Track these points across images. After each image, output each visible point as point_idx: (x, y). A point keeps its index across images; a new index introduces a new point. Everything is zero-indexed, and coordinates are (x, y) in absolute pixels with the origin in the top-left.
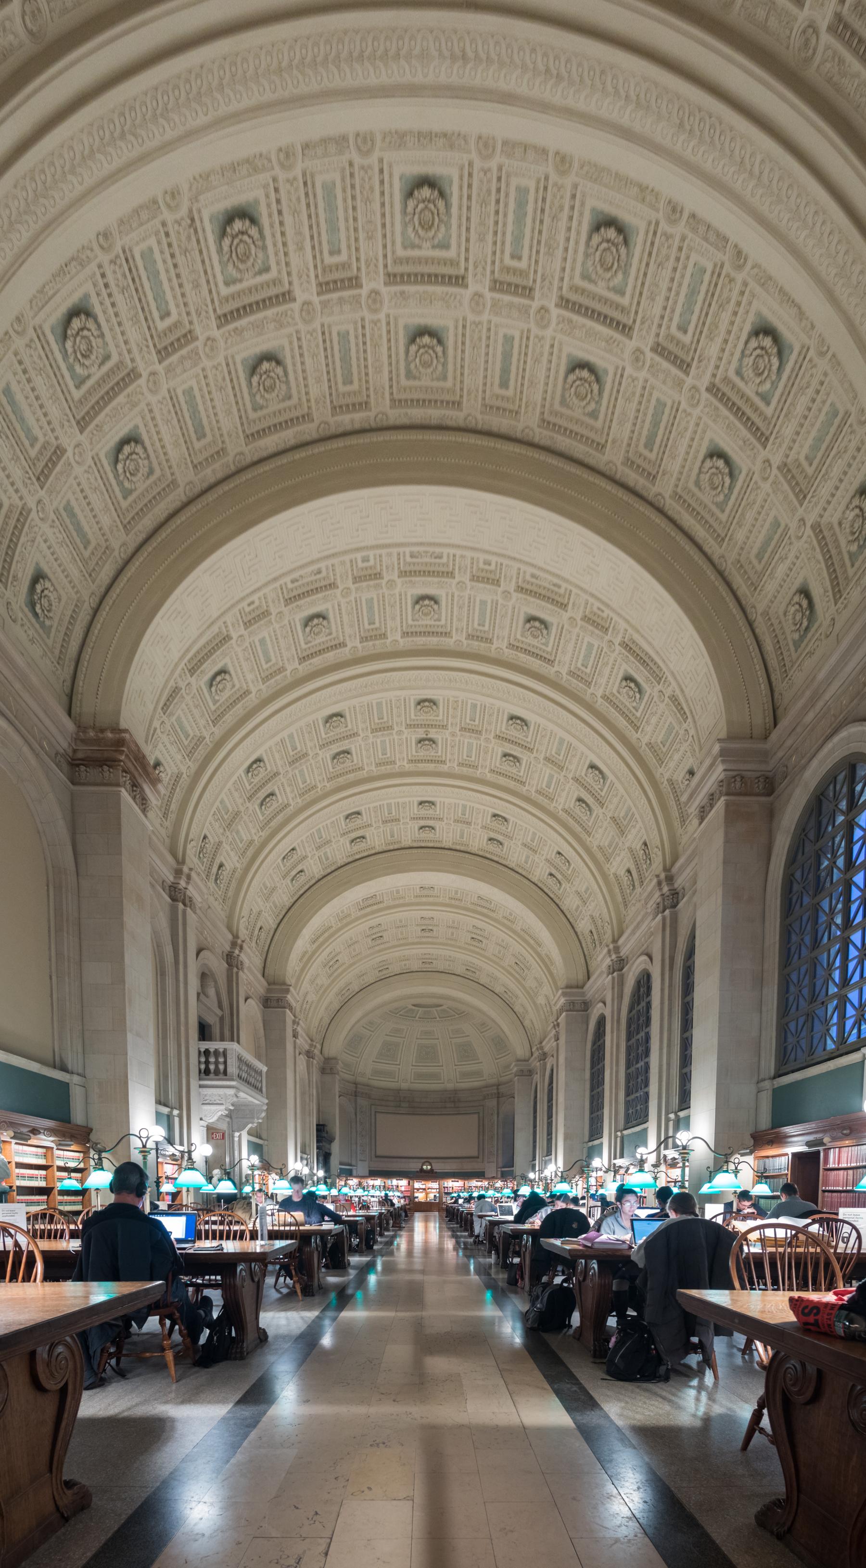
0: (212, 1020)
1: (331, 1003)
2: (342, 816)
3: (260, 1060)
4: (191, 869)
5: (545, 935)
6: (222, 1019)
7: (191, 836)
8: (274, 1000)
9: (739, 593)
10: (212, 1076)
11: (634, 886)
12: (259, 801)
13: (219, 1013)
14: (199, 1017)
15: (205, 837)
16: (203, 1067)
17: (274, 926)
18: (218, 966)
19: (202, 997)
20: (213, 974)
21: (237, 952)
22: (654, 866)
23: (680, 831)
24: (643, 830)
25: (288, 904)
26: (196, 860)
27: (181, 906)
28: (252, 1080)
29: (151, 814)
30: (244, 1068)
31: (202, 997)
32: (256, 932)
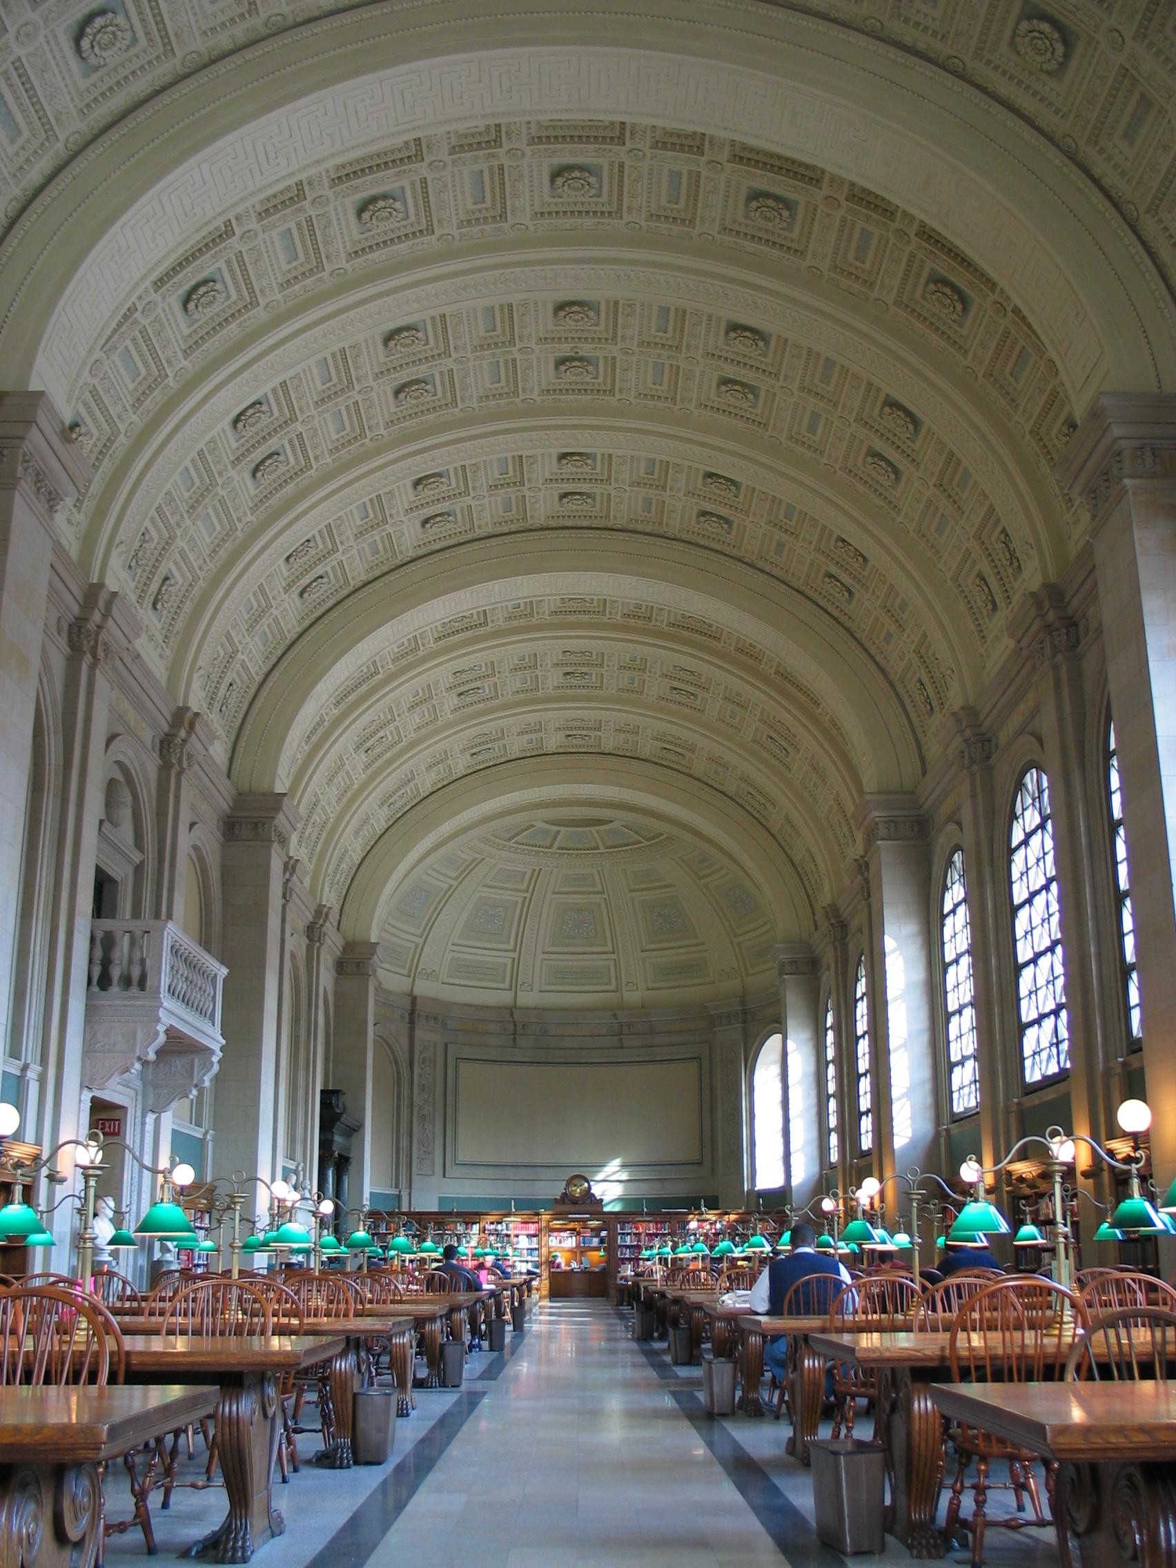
0: (121, 871)
1: (366, 820)
2: (408, 482)
3: (208, 949)
5: (824, 684)
6: (139, 869)
7: (120, 536)
8: (251, 821)
9: (1107, 182)
10: (115, 989)
11: (994, 604)
13: (137, 857)
14: (97, 866)
16: (97, 971)
17: (258, 679)
18: (147, 766)
19: (106, 824)
20: (130, 781)
22: (1026, 573)
25: (290, 637)
26: (125, 575)
28: (196, 996)
30: (183, 969)
31: (106, 824)
32: (222, 692)
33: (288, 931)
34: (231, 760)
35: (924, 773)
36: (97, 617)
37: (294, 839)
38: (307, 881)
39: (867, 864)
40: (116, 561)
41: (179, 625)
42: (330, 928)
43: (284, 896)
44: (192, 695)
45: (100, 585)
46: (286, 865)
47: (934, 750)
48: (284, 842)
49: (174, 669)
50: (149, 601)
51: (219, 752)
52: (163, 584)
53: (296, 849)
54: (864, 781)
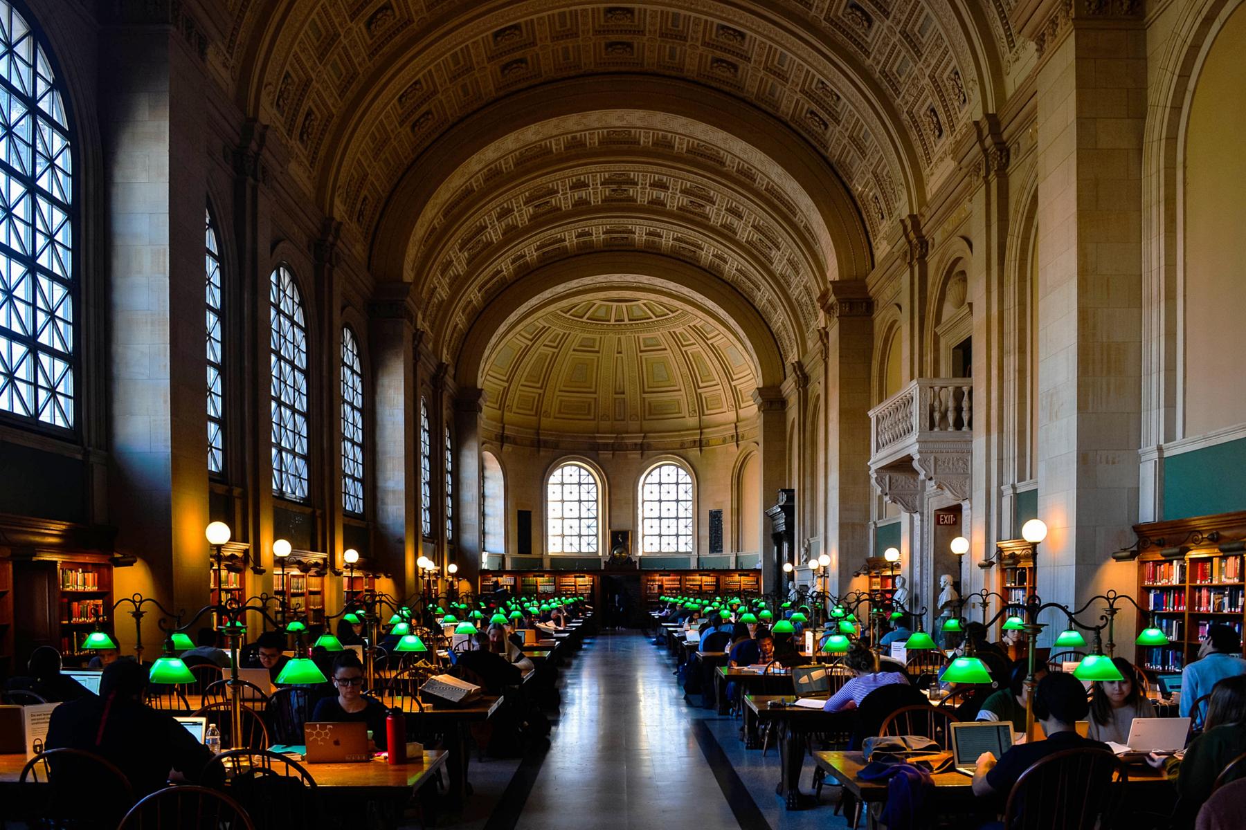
4: (266, 127)
12: (366, 18)
15: (287, 75)
21: (331, 239)
23: (1008, 56)
24: (951, 52)
27: (251, 180)
29: (211, 52)
32: (358, 206)
33: (419, 382)
34: (370, 258)
35: (873, 267)
36: (254, 146)
37: (420, 316)
38: (430, 346)
39: (827, 334)
40: (265, 100)
41: (322, 153)
42: (449, 381)
43: (415, 358)
44: (335, 210)
45: (255, 119)
46: (414, 335)
47: (882, 250)
48: (413, 319)
49: (320, 188)
50: (297, 132)
51: (359, 250)
52: (306, 119)
53: (423, 324)
54: (828, 275)
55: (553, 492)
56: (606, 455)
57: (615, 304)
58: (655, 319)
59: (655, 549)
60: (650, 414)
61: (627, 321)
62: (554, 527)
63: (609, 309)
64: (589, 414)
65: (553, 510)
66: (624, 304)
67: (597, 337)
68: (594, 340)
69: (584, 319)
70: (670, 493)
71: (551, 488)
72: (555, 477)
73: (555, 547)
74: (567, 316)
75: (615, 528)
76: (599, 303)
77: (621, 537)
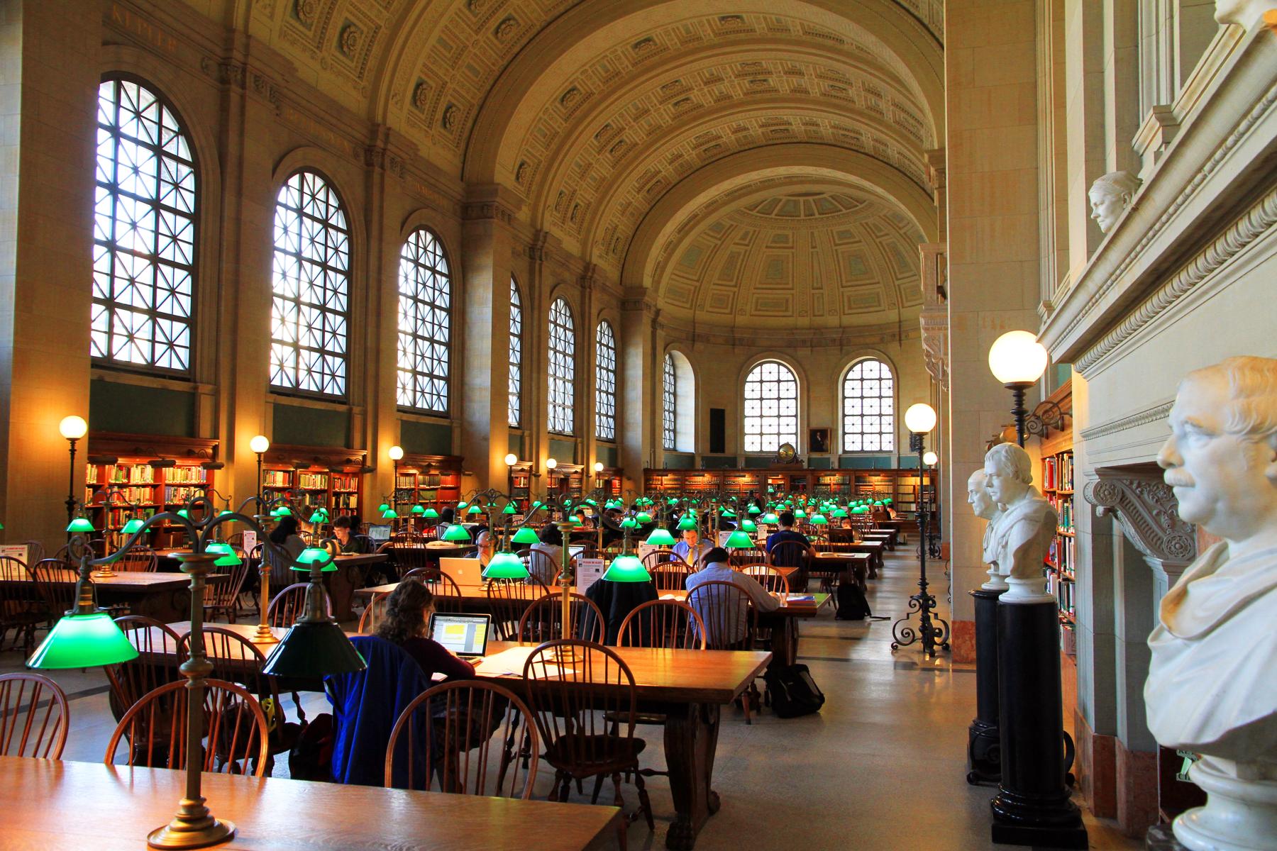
55: (750, 390)
56: (803, 353)
57: (802, 199)
58: (844, 211)
59: (857, 447)
60: (850, 308)
61: (817, 216)
62: (750, 425)
63: (796, 203)
64: (786, 310)
65: (750, 408)
66: (811, 198)
67: (790, 233)
68: (787, 237)
69: (773, 216)
70: (871, 388)
71: (748, 387)
72: (755, 375)
73: (751, 445)
74: (754, 213)
75: (814, 425)
76: (784, 199)
77: (819, 438)
